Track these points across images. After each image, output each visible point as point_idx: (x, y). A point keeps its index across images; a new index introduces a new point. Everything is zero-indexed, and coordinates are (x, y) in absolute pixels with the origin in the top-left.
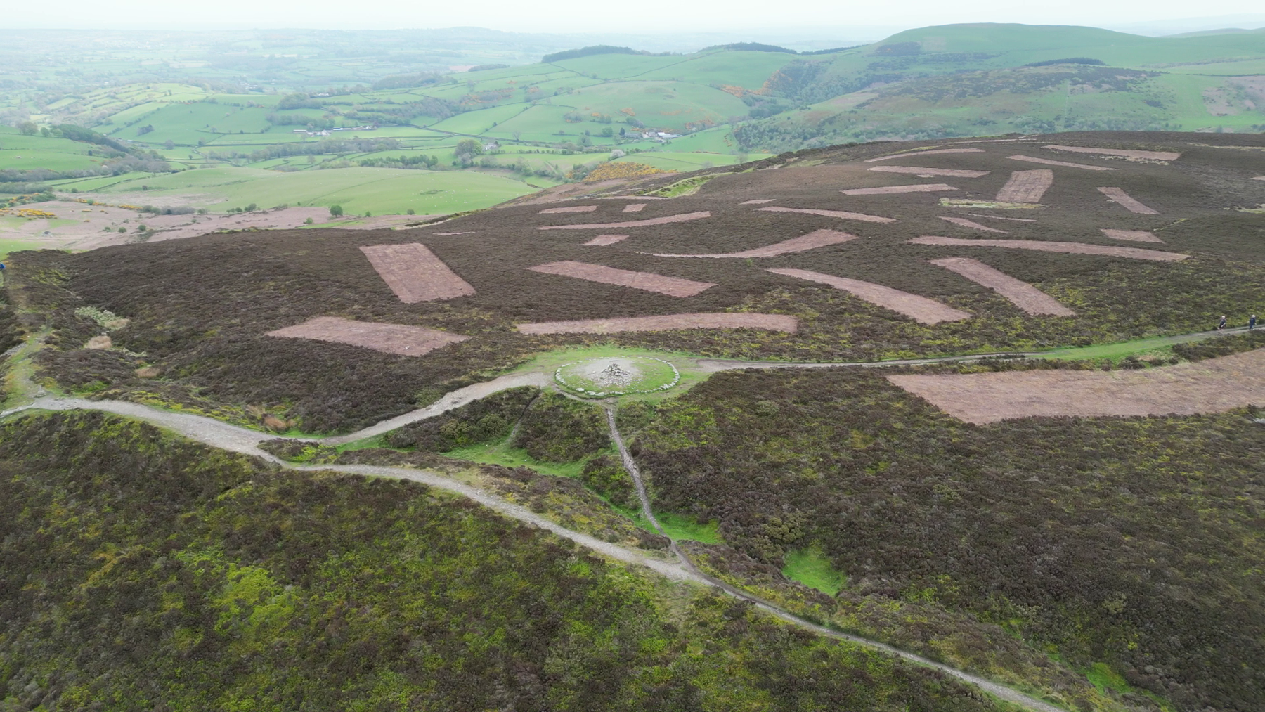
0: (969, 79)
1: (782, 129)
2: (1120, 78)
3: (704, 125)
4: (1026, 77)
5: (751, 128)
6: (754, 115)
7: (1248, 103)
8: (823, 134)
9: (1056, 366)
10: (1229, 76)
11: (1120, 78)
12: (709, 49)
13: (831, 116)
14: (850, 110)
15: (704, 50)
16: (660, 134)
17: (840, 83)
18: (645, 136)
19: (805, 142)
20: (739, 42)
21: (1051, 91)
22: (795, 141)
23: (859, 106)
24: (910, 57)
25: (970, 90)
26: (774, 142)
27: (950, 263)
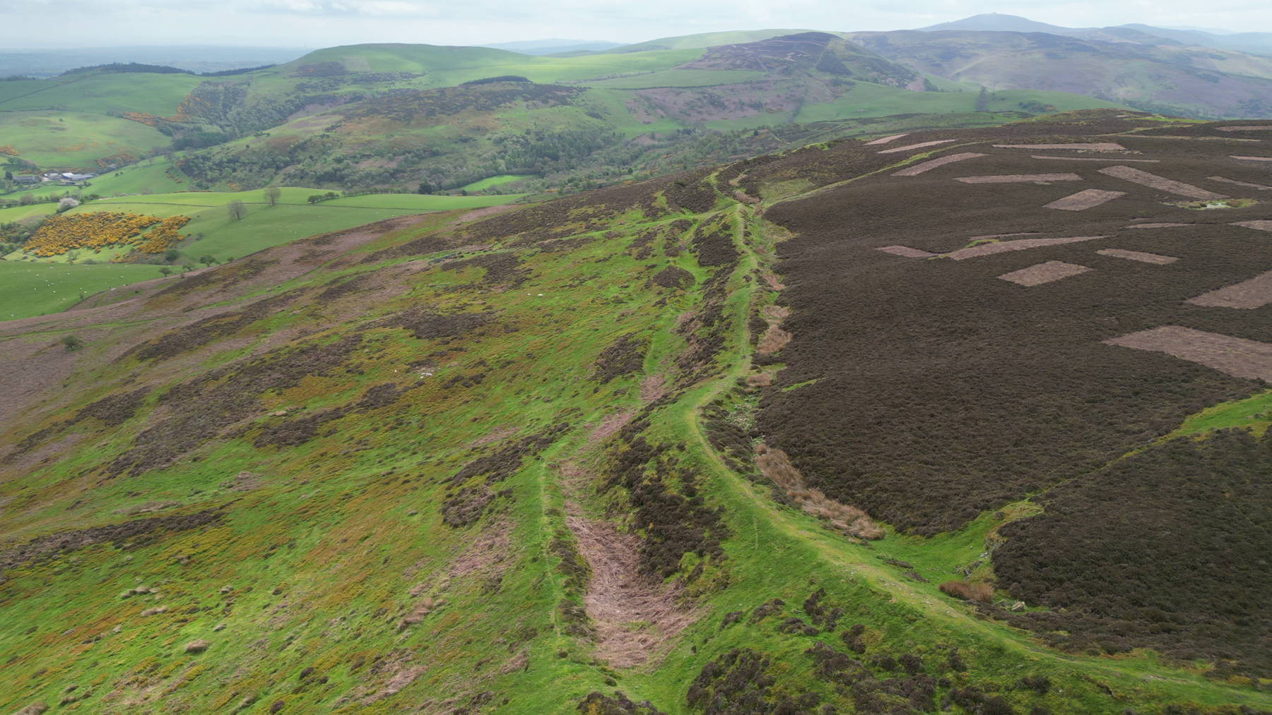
0: (429, 98)
2: (559, 93)
3: (124, 160)
4: (482, 94)
5: (201, 160)
6: (180, 146)
7: (661, 112)
8: (299, 162)
10: (636, 89)
11: (559, 93)
12: (76, 71)
13: (301, 141)
14: (321, 133)
15: (68, 73)
16: (65, 174)
17: (270, 107)
18: (45, 180)
19: (279, 172)
20: (112, 63)
21: (510, 107)
23: (328, 130)
24: (338, 77)
25: (437, 109)
26: (239, 174)
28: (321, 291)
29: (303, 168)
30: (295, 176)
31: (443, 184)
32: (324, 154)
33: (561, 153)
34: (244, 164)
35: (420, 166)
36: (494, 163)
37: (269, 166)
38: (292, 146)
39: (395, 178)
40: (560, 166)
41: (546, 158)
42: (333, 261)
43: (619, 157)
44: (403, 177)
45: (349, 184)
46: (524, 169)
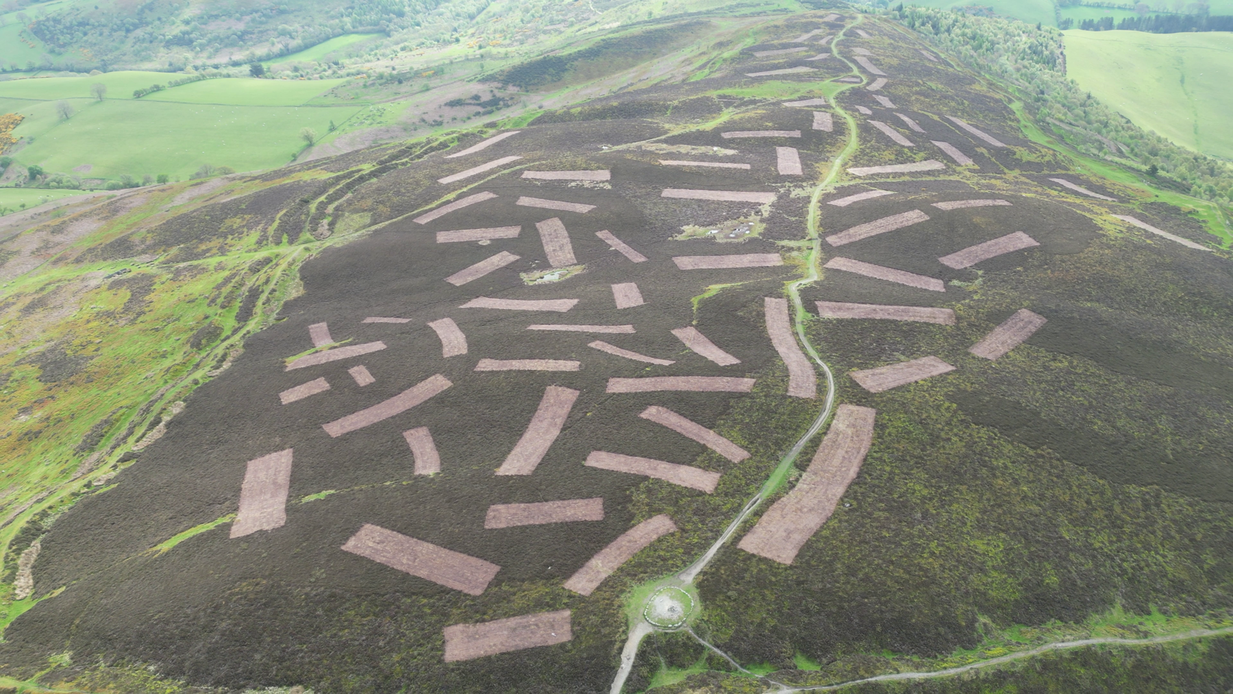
1: (92, 21)
5: (52, 23)
8: (147, 24)
9: (771, 501)
22: (116, 35)
27: (652, 413)
28: (28, 300)
29: (152, 30)
30: (144, 40)
31: (290, 47)
32: (172, 14)
33: (407, 9)
34: (94, 27)
35: (267, 27)
36: (341, 21)
37: (119, 29)
38: (139, 7)
39: (243, 40)
40: (406, 24)
41: (392, 15)
42: (58, 256)
43: (465, 10)
44: (251, 39)
45: (198, 49)
46: (369, 27)
